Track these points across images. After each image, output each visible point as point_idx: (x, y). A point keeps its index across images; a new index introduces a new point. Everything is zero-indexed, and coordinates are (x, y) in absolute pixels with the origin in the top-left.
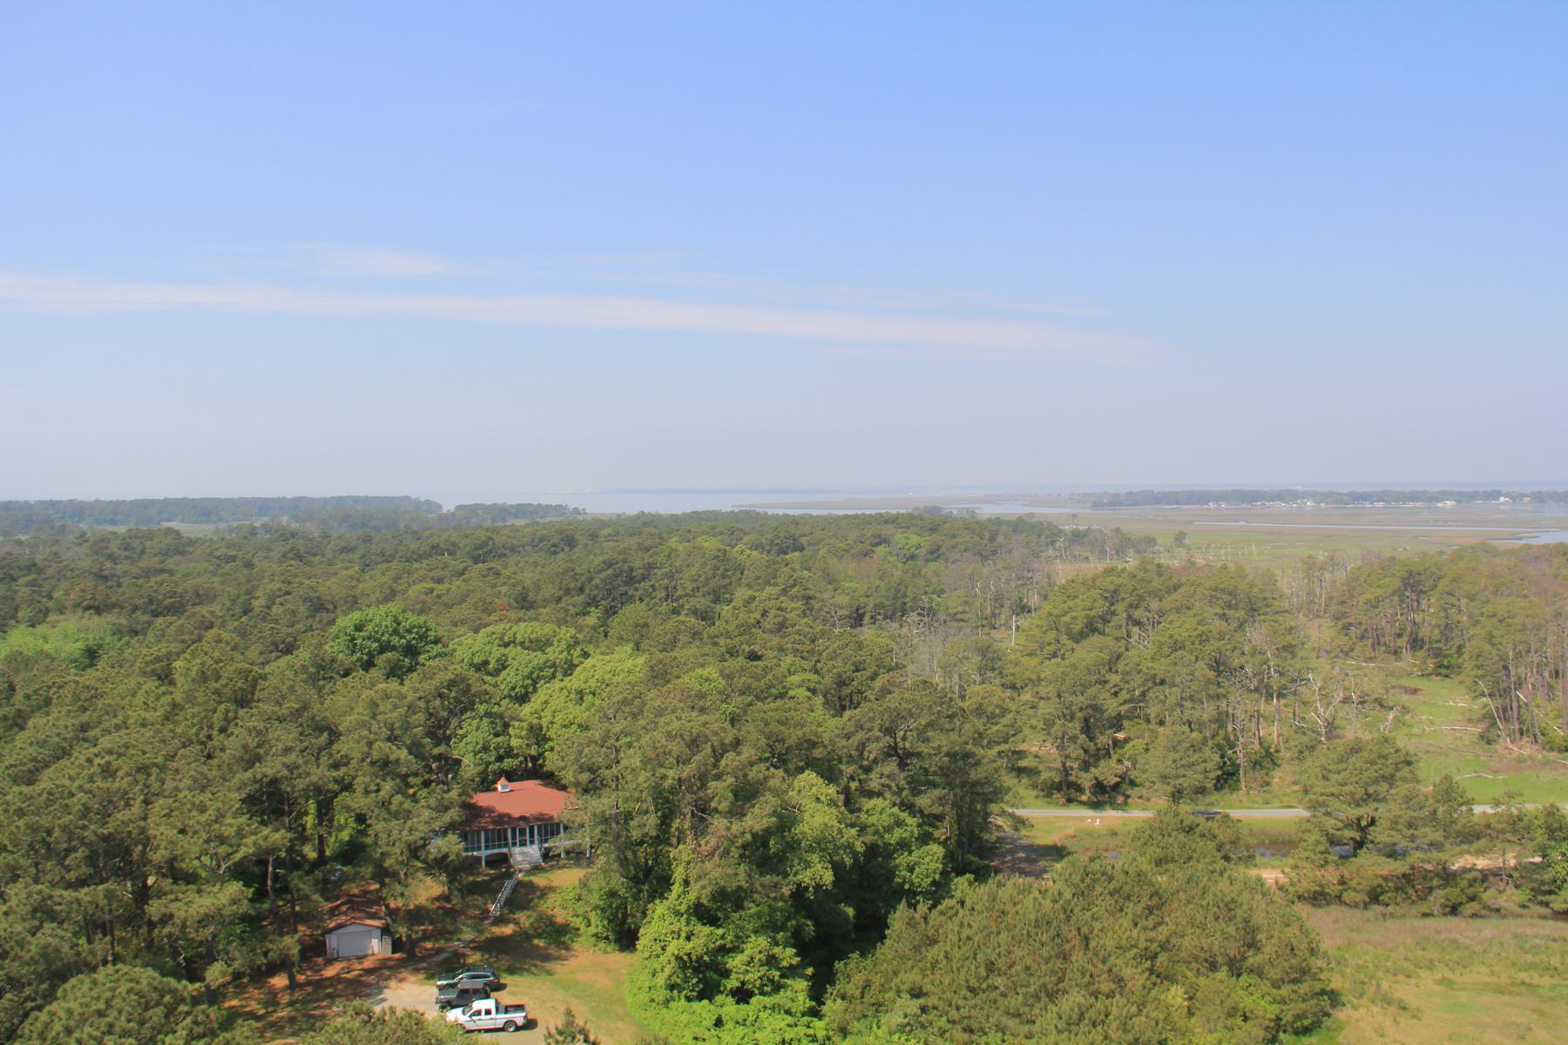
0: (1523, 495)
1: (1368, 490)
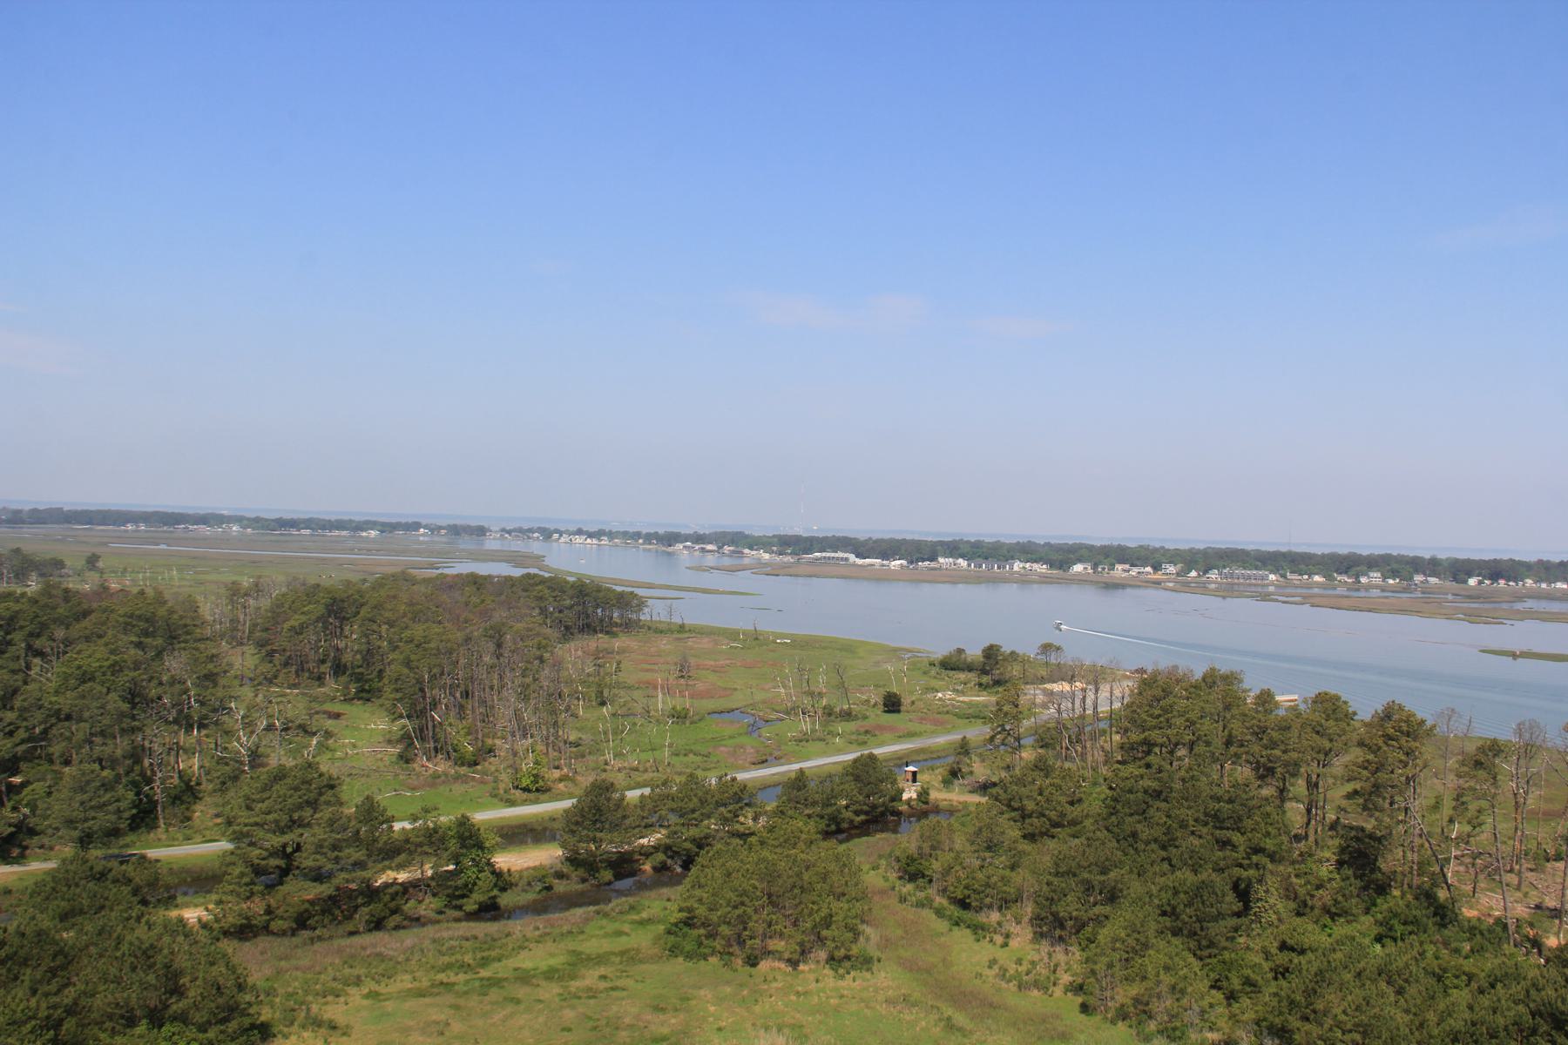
0: (441, 528)
1: (295, 516)
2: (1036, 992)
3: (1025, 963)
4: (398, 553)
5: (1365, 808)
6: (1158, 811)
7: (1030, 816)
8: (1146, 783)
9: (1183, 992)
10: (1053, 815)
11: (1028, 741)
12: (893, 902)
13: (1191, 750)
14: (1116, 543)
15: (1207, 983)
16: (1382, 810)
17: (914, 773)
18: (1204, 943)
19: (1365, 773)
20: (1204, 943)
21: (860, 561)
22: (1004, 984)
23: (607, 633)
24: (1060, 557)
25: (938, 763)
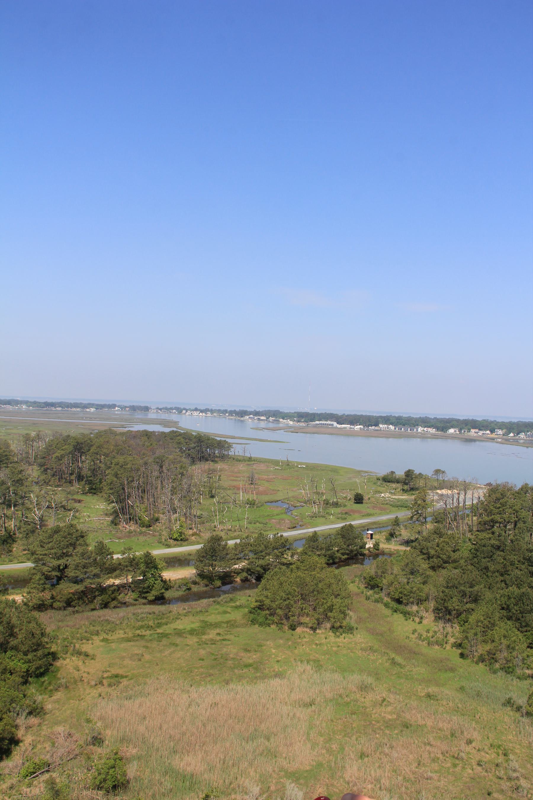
0: (126, 407)
1: (54, 401)
2: (437, 647)
3: (431, 632)
4: (107, 419)
6: (499, 556)
7: (432, 557)
8: (492, 542)
9: (513, 649)
10: (444, 557)
11: (429, 519)
12: (363, 599)
13: (515, 525)
14: (471, 418)
15: (526, 645)
17: (372, 535)
18: (524, 624)
20: (524, 624)
21: (339, 426)
22: (420, 642)
23: (213, 461)
24: (442, 425)
25: (383, 529)
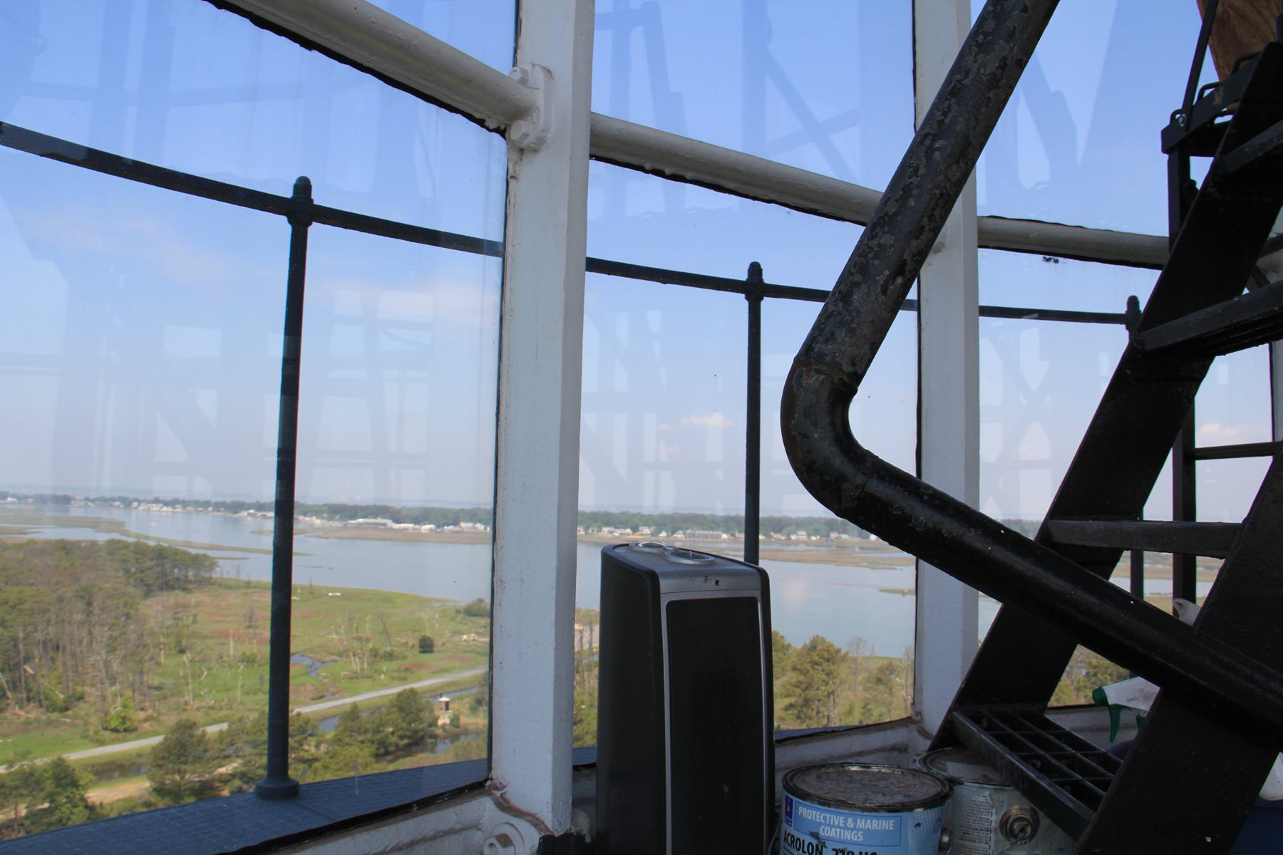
0: (27, 497)
5: (798, 717)
14: (602, 510)
16: (811, 718)
17: (447, 703)
19: (798, 691)
21: (396, 526)
23: (184, 589)
25: (465, 693)
